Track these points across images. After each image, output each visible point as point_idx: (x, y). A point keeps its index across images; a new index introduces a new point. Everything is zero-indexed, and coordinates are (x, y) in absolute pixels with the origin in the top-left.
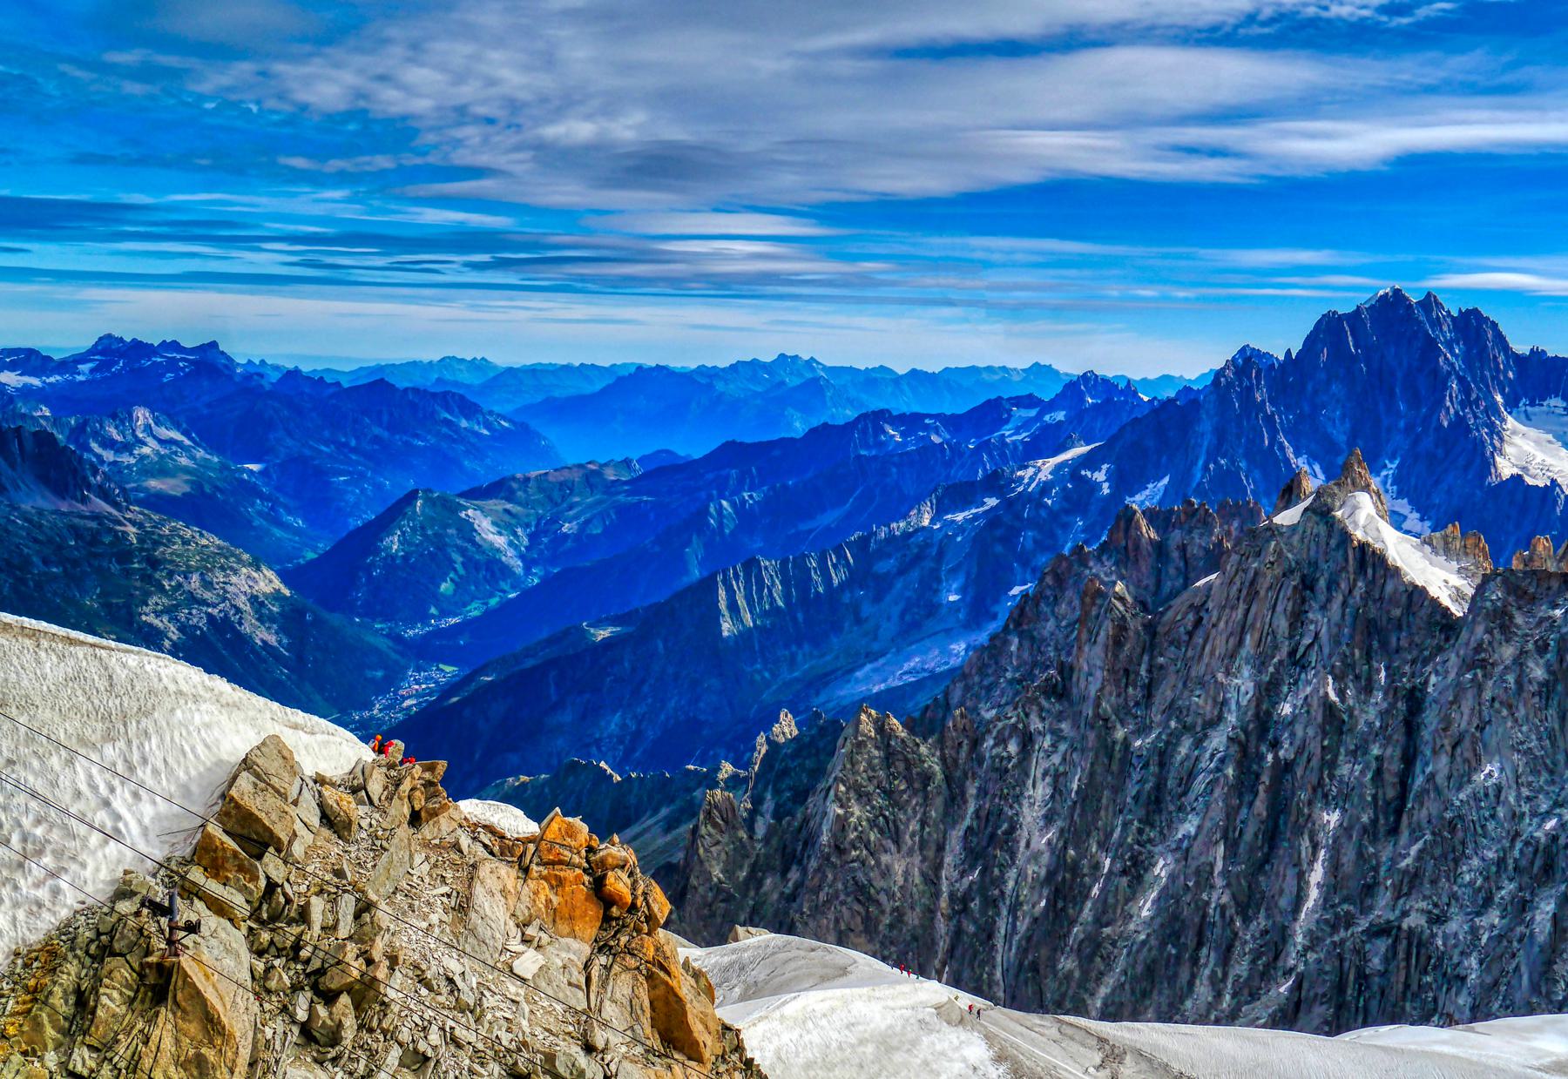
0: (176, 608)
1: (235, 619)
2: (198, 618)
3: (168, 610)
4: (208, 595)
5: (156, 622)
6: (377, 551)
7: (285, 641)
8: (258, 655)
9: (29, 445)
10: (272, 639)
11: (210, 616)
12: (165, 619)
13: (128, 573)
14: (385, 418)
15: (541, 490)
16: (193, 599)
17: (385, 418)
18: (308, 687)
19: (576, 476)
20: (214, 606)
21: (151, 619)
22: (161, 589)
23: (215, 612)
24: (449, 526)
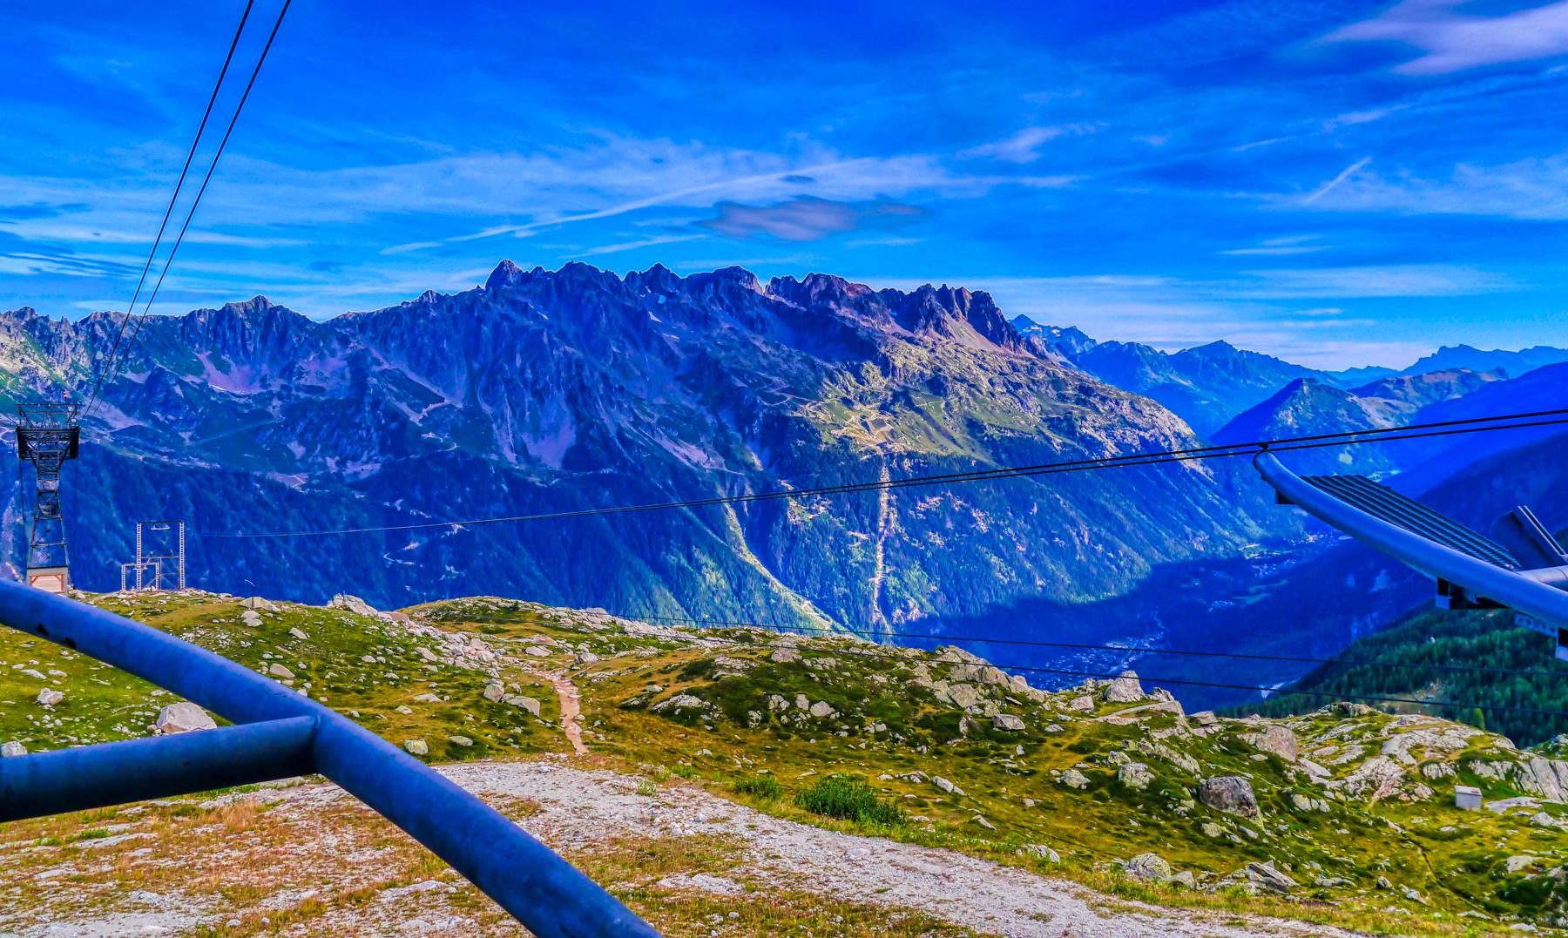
0: (1113, 427)
1: (1165, 445)
2: (1132, 438)
3: (1109, 430)
4: (1138, 421)
5: (1096, 435)
6: (1273, 422)
7: (1211, 472)
8: (1190, 479)
9: (968, 298)
10: (1200, 469)
11: (1143, 441)
12: (1103, 434)
13: (1063, 398)
14: (1231, 365)
15: (1417, 388)
16: (1125, 422)
17: (1231, 365)
18: (1241, 513)
19: (1452, 379)
20: (1146, 430)
21: (1090, 432)
22: (1097, 410)
23: (1147, 436)
24: (1336, 407)
